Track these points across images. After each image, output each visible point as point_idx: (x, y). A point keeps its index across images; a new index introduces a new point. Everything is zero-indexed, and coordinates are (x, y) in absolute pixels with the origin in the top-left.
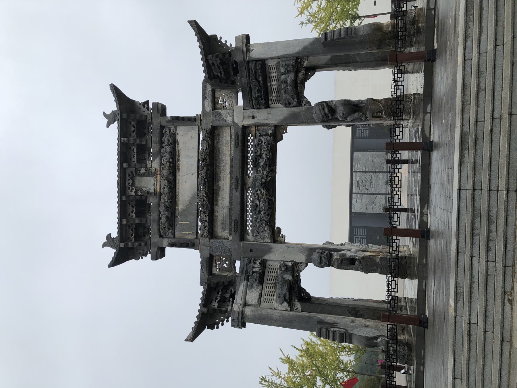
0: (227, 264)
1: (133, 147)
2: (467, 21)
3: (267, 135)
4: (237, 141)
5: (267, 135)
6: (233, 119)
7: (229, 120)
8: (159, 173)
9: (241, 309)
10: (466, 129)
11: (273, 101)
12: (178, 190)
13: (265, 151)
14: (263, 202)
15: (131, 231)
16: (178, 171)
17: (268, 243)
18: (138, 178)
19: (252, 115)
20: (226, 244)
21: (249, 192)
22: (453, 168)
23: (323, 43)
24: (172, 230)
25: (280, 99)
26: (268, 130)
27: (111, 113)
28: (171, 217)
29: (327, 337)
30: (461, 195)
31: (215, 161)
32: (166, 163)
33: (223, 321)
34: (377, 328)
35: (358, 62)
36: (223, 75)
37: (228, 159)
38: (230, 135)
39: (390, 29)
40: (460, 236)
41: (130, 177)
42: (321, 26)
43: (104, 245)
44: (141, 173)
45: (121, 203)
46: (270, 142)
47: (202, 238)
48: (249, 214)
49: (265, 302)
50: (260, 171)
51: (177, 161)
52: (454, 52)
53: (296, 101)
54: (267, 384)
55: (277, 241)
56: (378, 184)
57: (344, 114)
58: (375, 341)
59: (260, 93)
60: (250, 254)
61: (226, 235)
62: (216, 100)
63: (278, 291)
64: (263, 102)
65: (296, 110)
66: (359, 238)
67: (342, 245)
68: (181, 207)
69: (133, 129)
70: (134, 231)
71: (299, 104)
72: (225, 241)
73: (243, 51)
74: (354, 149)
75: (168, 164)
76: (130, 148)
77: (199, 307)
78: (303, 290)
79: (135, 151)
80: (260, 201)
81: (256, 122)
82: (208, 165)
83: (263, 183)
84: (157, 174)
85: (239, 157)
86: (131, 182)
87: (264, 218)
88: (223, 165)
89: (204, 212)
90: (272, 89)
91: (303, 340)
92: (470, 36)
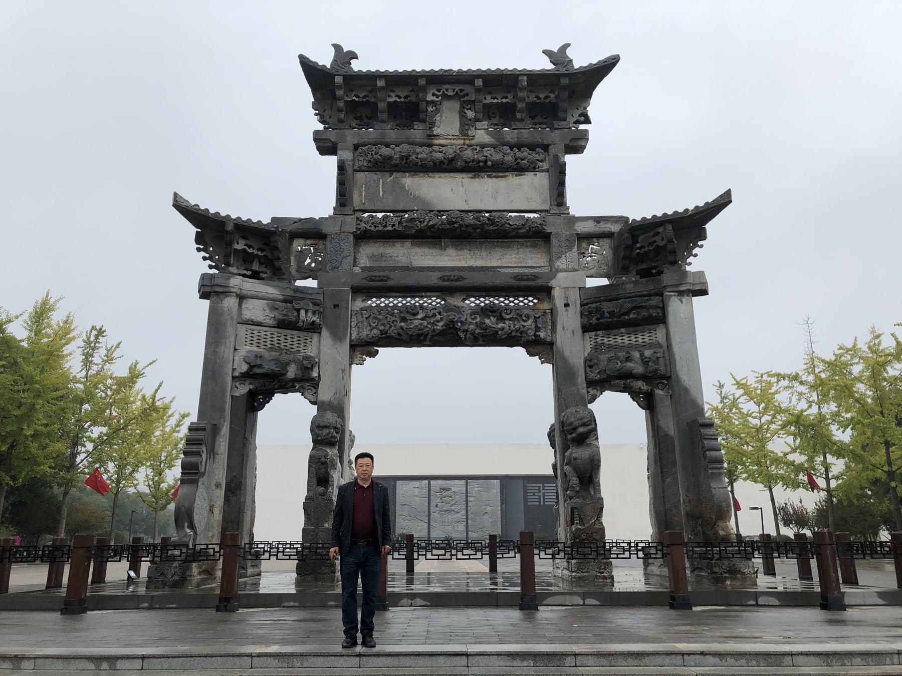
0: (310, 264)
1: (510, 96)
2: (747, 656)
3: (537, 329)
4: (525, 278)
5: (537, 329)
6: (562, 271)
7: (561, 264)
8: (467, 142)
9: (233, 290)
10: (570, 661)
11: (596, 339)
12: (438, 176)
13: (510, 327)
14: (421, 324)
15: (365, 93)
16: (470, 176)
17: (351, 334)
18: (456, 105)
19: (570, 302)
20: (346, 261)
21: (438, 301)
22: (501, 642)
23: (695, 421)
24: (369, 167)
25: (598, 350)
26: (545, 331)
27: (569, 58)
28: (391, 165)
30: (458, 658)
31: (489, 240)
32: (485, 154)
34: (209, 527)
35: (663, 480)
36: (638, 251)
37: (494, 263)
38: (535, 265)
39: (721, 533)
40: (389, 658)
41: (459, 92)
43: (338, 48)
44: (466, 111)
45: (413, 76)
46: (524, 335)
47: (355, 219)
48: (399, 302)
49: (246, 333)
50: (476, 318)
51: (488, 173)
52: (693, 638)
53: (596, 378)
54: (92, 339)
55: (354, 351)
56: (446, 524)
57: (575, 459)
58: (186, 524)
59: (608, 315)
60: (329, 305)
61: (362, 262)
62: (595, 240)
63: (267, 355)
64: (594, 321)
68: (408, 181)
69: (542, 96)
70: (364, 100)
72: (350, 259)
73: (679, 285)
74: (506, 481)
75: (483, 158)
76: (509, 92)
77: (234, 217)
78: (268, 397)
79: (505, 100)
80: (422, 319)
81: (559, 310)
82: (482, 229)
83: (454, 325)
84: (464, 139)
85: (498, 282)
86: (450, 93)
87: (393, 328)
88: (484, 254)
89: (400, 223)
90: (616, 337)
91: (171, 402)
92: (723, 661)
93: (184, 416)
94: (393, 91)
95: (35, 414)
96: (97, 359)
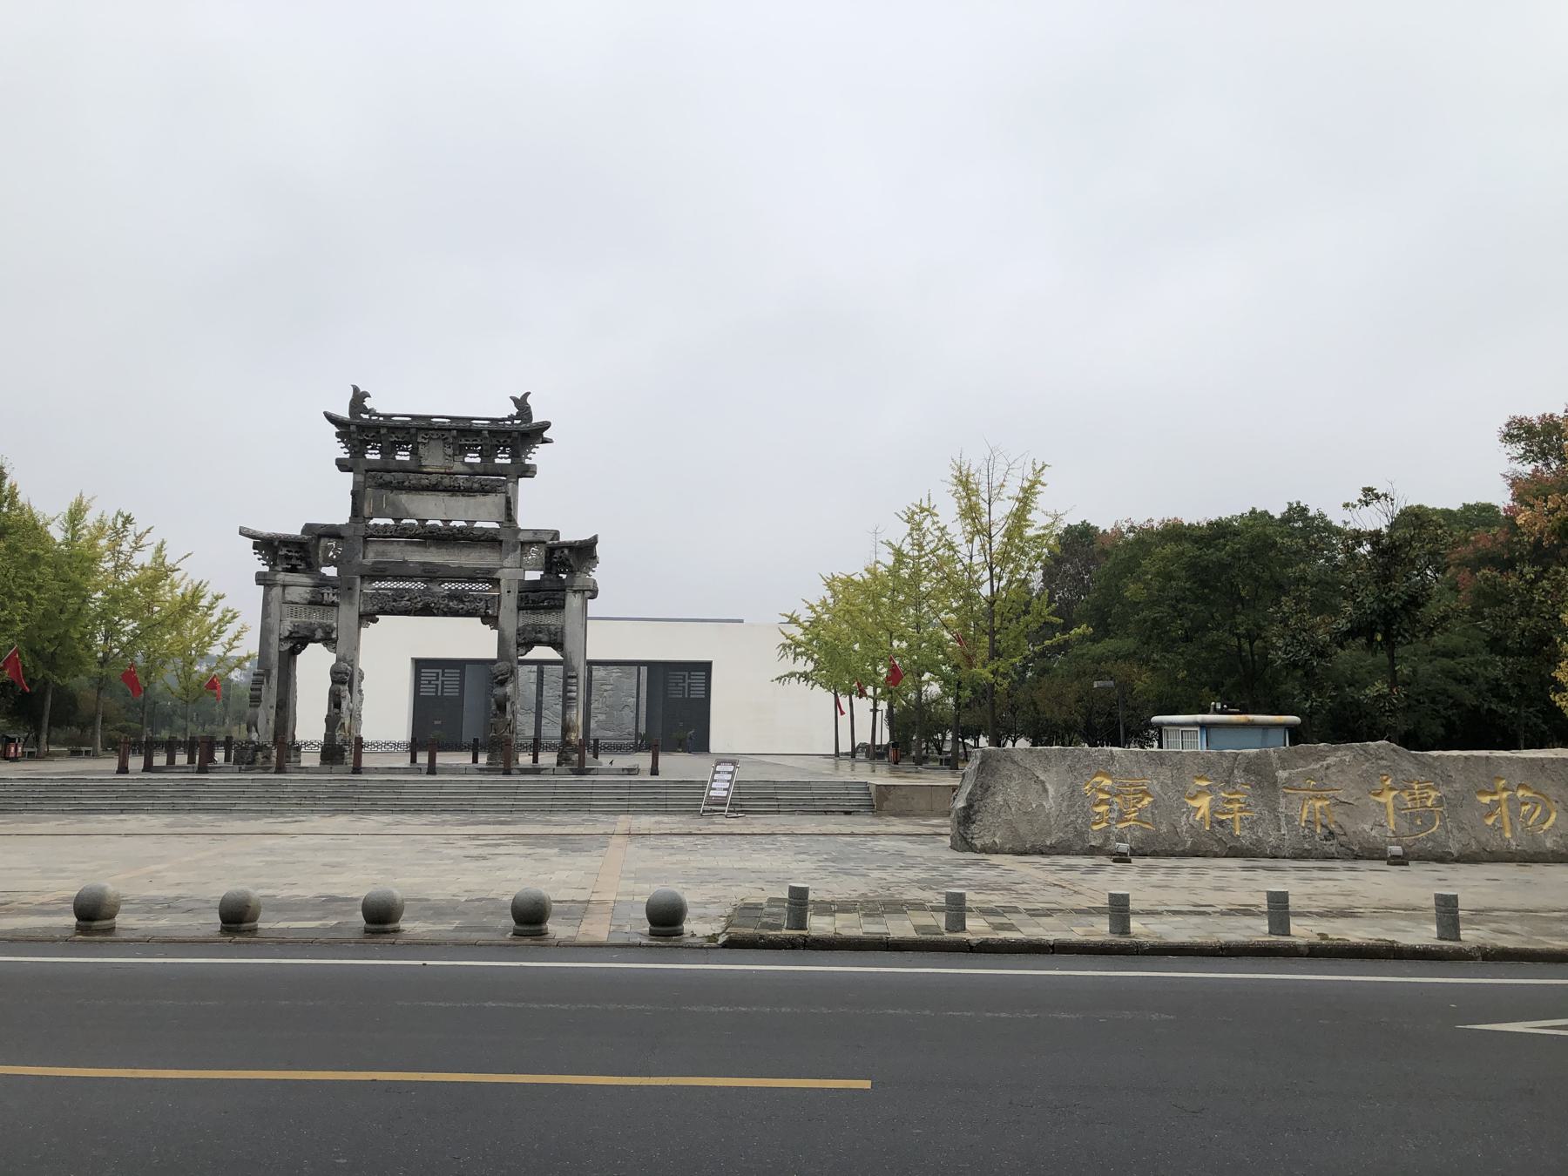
0: (332, 556)
3: (487, 608)
5: (487, 608)
15: (373, 434)
16: (450, 494)
29: (254, 682)
33: (264, 559)
34: (266, 732)
42: (823, 614)
43: (356, 389)
48: (395, 585)
54: (119, 525)
64: (523, 605)
65: (513, 643)
66: (437, 680)
67: (360, 691)
68: (405, 499)
69: (502, 441)
71: (519, 645)
74: (651, 665)
76: (478, 436)
78: (304, 646)
80: (408, 600)
86: (435, 437)
88: (456, 551)
89: (396, 530)
93: (217, 598)
94: (394, 433)
95: (81, 619)
96: (125, 547)
